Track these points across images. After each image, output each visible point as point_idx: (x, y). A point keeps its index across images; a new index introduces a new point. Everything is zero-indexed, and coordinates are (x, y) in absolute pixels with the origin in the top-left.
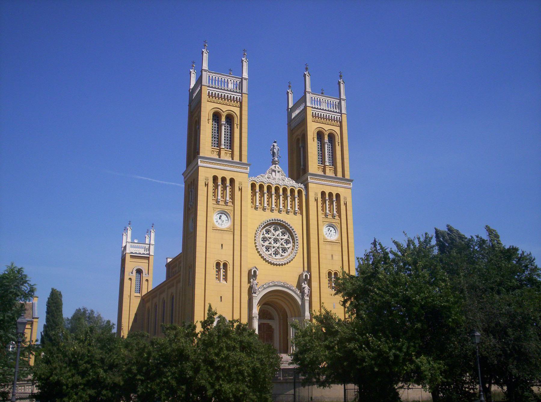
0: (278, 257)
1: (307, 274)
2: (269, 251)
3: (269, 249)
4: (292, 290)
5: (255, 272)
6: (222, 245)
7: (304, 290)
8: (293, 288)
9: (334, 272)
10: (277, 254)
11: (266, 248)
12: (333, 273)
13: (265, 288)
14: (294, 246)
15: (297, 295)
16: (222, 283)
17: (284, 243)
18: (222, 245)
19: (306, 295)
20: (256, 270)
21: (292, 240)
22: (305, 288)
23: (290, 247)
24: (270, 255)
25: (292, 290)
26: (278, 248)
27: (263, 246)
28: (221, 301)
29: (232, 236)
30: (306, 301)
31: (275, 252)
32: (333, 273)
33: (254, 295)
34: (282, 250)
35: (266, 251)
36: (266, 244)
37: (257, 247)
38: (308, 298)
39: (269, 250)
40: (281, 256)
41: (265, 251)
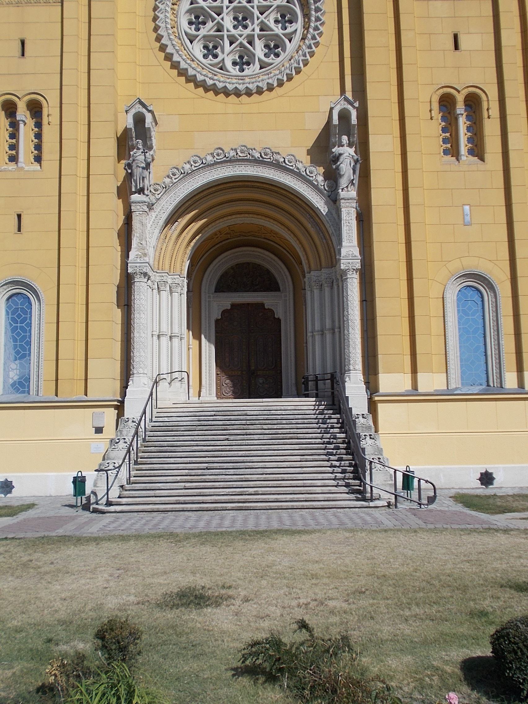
0: (255, 68)
1: (350, 107)
2: (216, 56)
3: (215, 47)
4: (298, 175)
5: (139, 120)
6: (23, 43)
7: (338, 168)
8: (300, 165)
9: (465, 92)
10: (248, 64)
11: (206, 47)
12: (460, 98)
13: (186, 175)
14: (306, 27)
15: (316, 187)
16: (22, 168)
17: (272, 24)
18: (23, 43)
19: (344, 182)
20: (144, 111)
21: (302, 10)
22: (341, 159)
23: (296, 30)
24: (221, 68)
25: (298, 175)
26: (250, 43)
27: (191, 42)
28: (19, 230)
29: (60, 8)
30: (343, 203)
31: (241, 57)
32: (460, 98)
33: (135, 197)
34: (267, 46)
35: (205, 56)
36: (208, 29)
37: (164, 41)
38: (353, 193)
39: (218, 51)
40: (261, 68)
41: (201, 58)
